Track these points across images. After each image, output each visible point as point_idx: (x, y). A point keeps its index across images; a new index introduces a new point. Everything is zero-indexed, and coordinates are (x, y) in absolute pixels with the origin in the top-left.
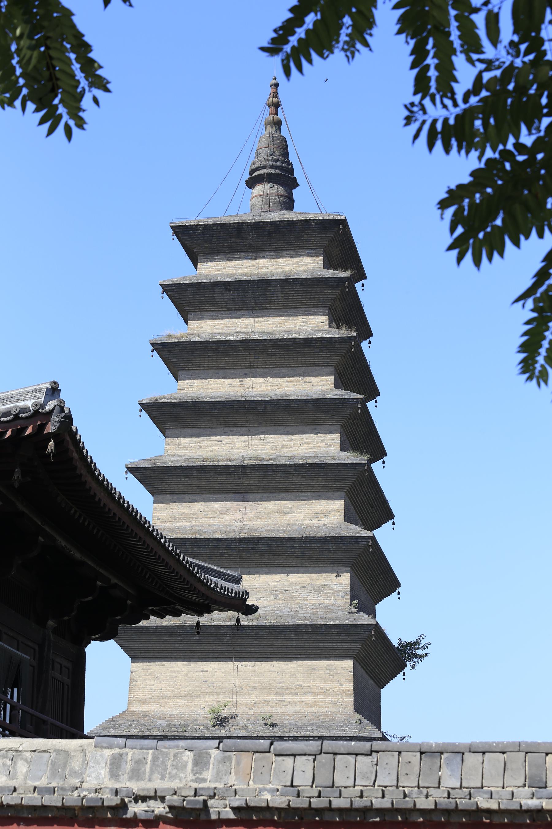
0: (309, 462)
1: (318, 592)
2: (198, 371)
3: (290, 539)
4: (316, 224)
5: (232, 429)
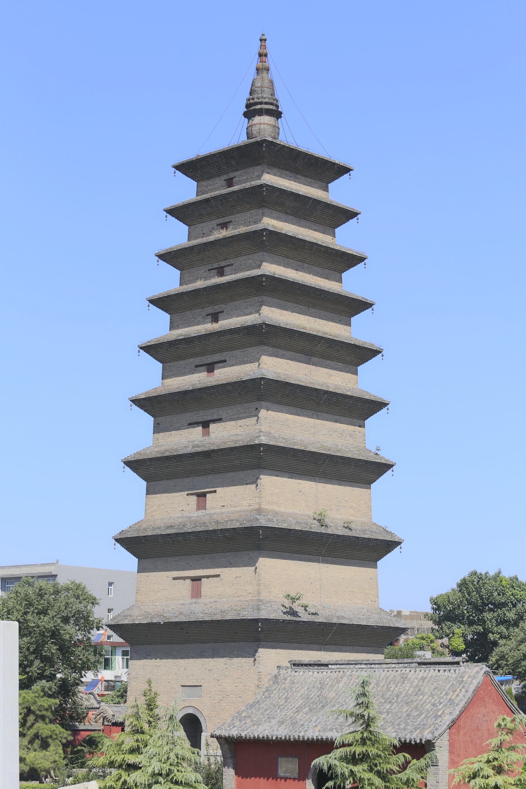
0: (356, 344)
1: (351, 436)
2: (273, 255)
3: (352, 397)
4: (338, 167)
5: (298, 305)
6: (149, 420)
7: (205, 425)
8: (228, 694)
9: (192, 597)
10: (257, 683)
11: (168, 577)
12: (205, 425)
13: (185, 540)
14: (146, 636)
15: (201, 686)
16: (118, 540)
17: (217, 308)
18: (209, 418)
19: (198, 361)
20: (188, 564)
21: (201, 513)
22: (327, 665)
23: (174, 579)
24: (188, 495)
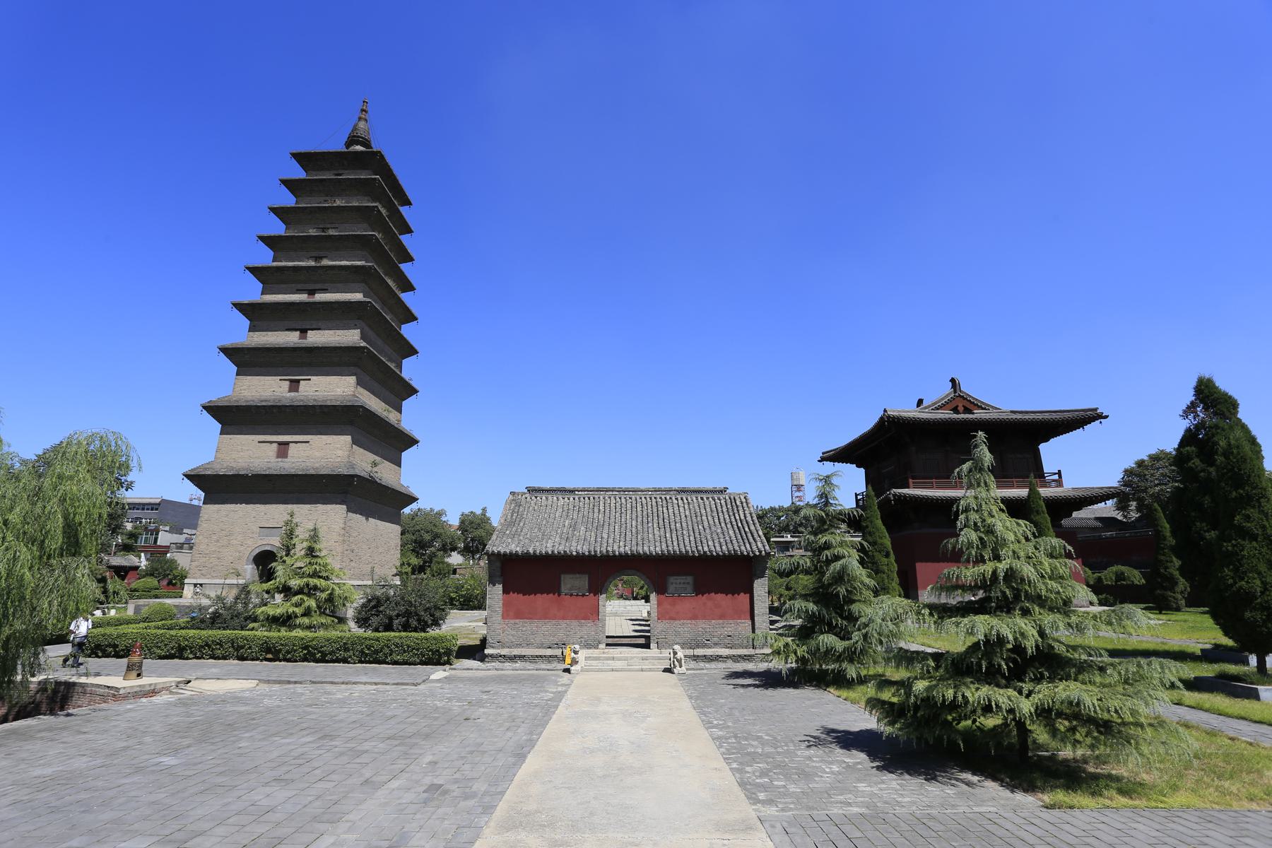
6: (246, 323)
7: (303, 332)
9: (278, 457)
12: (303, 332)
16: (205, 407)
17: (322, 254)
19: (299, 286)
21: (292, 394)
22: (572, 491)
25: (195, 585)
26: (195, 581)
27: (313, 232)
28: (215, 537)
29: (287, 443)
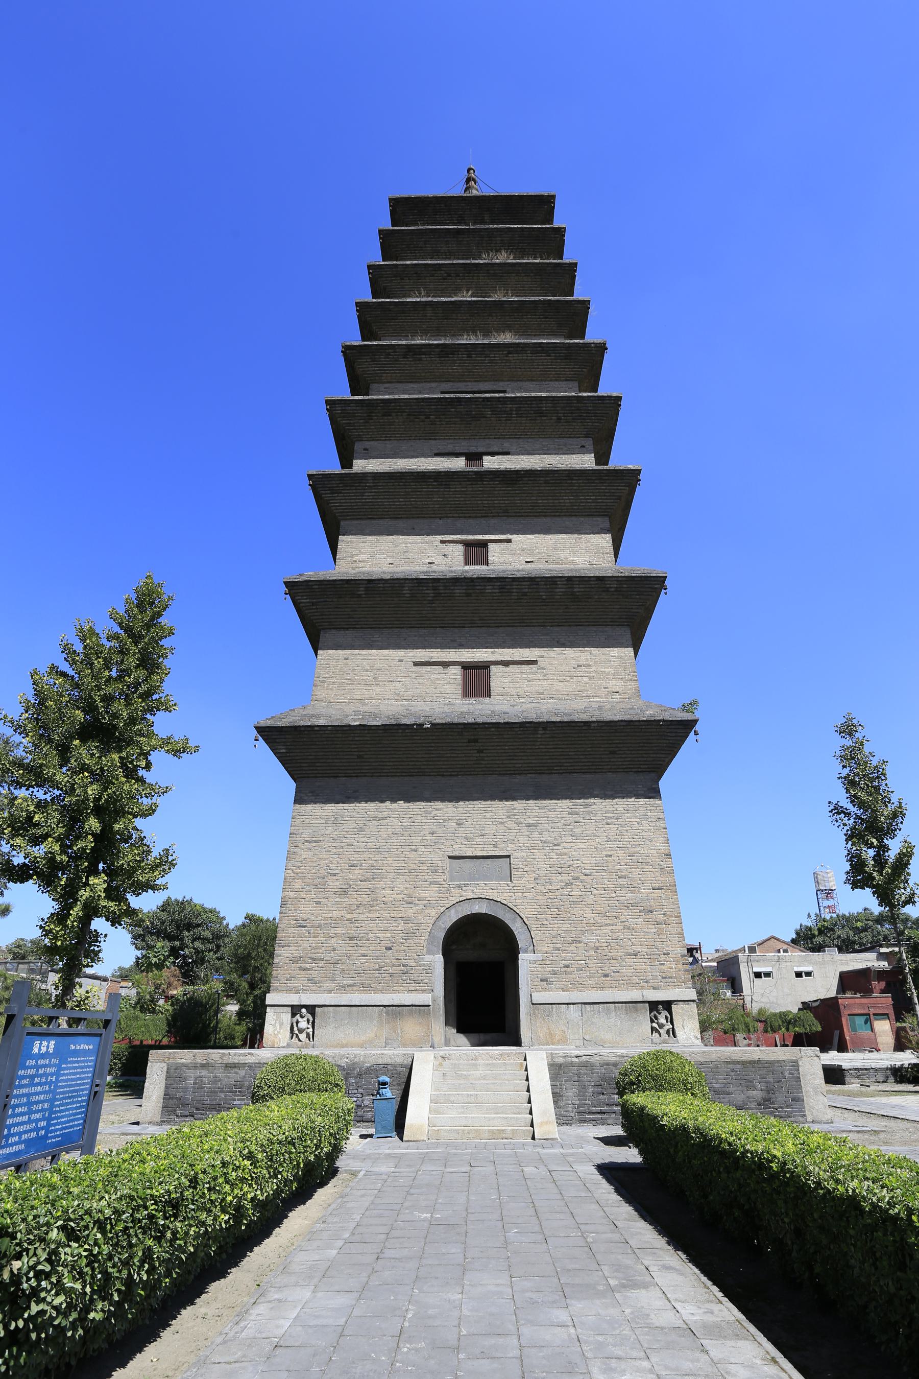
7: (474, 457)
8: (588, 871)
10: (663, 848)
11: (401, 661)
13: (468, 595)
14: (359, 757)
15: (509, 856)
18: (481, 450)
20: (455, 641)
23: (416, 664)
24: (442, 542)
25: (295, 1010)
26: (294, 999)
27: (467, 297)
28: (334, 884)
29: (484, 667)
